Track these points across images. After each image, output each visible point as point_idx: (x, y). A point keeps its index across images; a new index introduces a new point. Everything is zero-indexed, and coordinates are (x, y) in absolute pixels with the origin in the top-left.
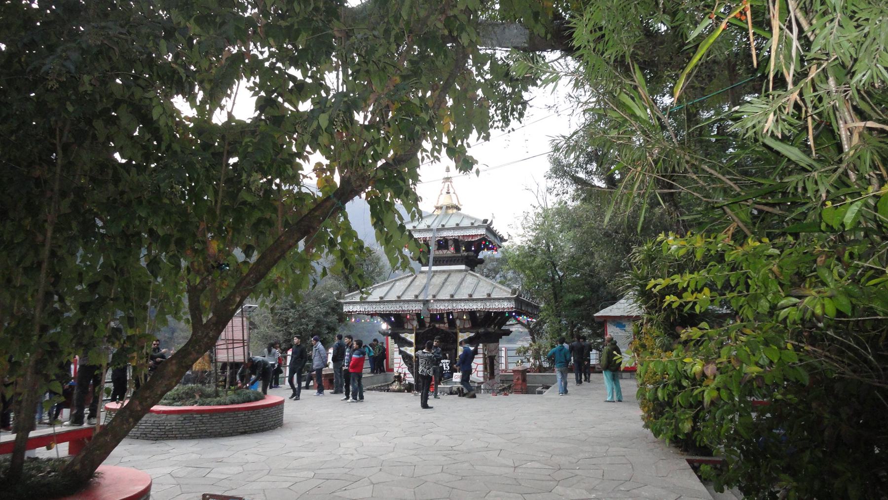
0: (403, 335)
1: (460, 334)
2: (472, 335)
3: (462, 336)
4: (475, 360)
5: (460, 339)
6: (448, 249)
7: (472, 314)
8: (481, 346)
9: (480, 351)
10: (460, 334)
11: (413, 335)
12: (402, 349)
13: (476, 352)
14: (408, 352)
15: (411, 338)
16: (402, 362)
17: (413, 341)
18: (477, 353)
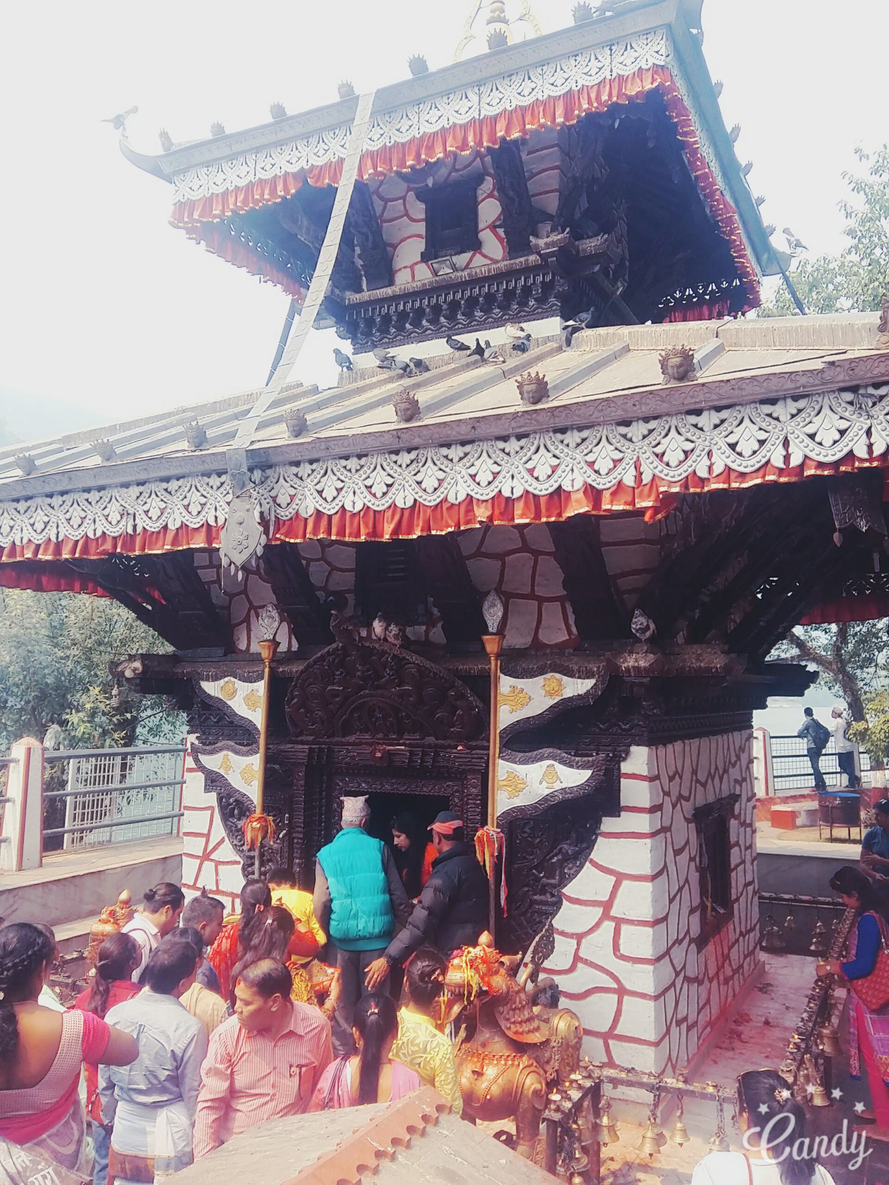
0: (210, 688)
1: (506, 683)
2: (577, 687)
3: (521, 698)
4: (604, 850)
5: (506, 715)
6: (476, 246)
7: (578, 544)
8: (638, 759)
9: (635, 793)
10: (506, 683)
11: (261, 687)
12: (209, 761)
13: (603, 798)
14: (236, 781)
15: (246, 699)
16: (219, 831)
17: (257, 717)
18: (614, 808)
